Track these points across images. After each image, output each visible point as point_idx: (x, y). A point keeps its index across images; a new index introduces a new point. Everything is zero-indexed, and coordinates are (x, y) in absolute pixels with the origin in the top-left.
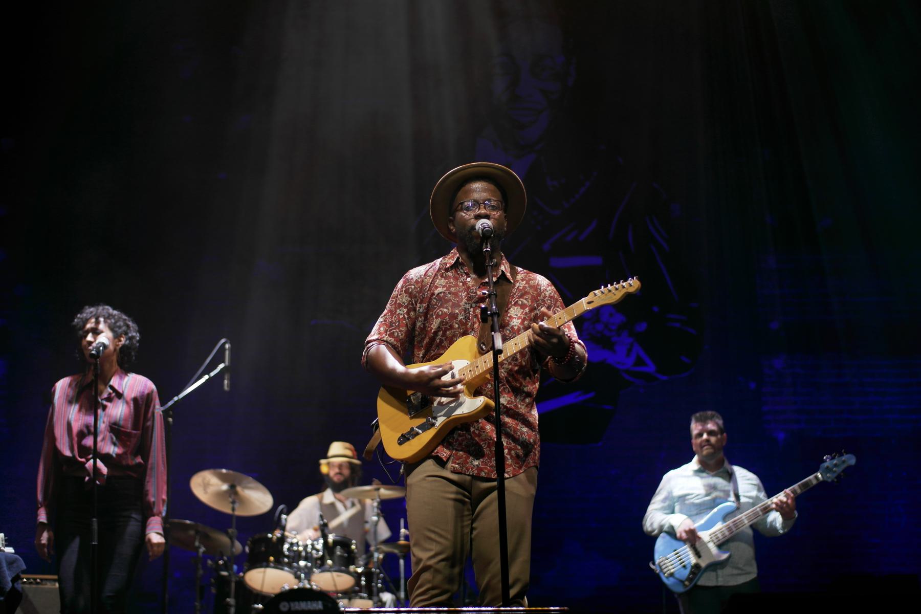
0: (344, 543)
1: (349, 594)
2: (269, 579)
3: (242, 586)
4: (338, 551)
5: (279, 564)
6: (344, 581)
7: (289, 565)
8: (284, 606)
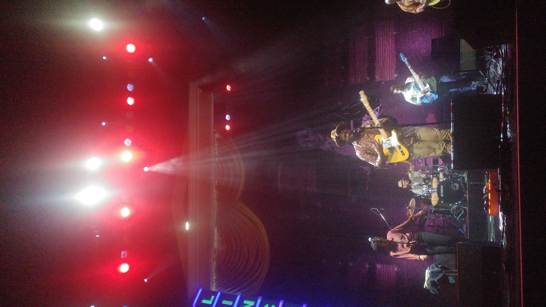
0: (424, 180)
1: (438, 179)
2: (434, 199)
3: (435, 207)
4: (427, 181)
5: (430, 197)
6: (435, 180)
7: (430, 194)
8: (442, 195)
